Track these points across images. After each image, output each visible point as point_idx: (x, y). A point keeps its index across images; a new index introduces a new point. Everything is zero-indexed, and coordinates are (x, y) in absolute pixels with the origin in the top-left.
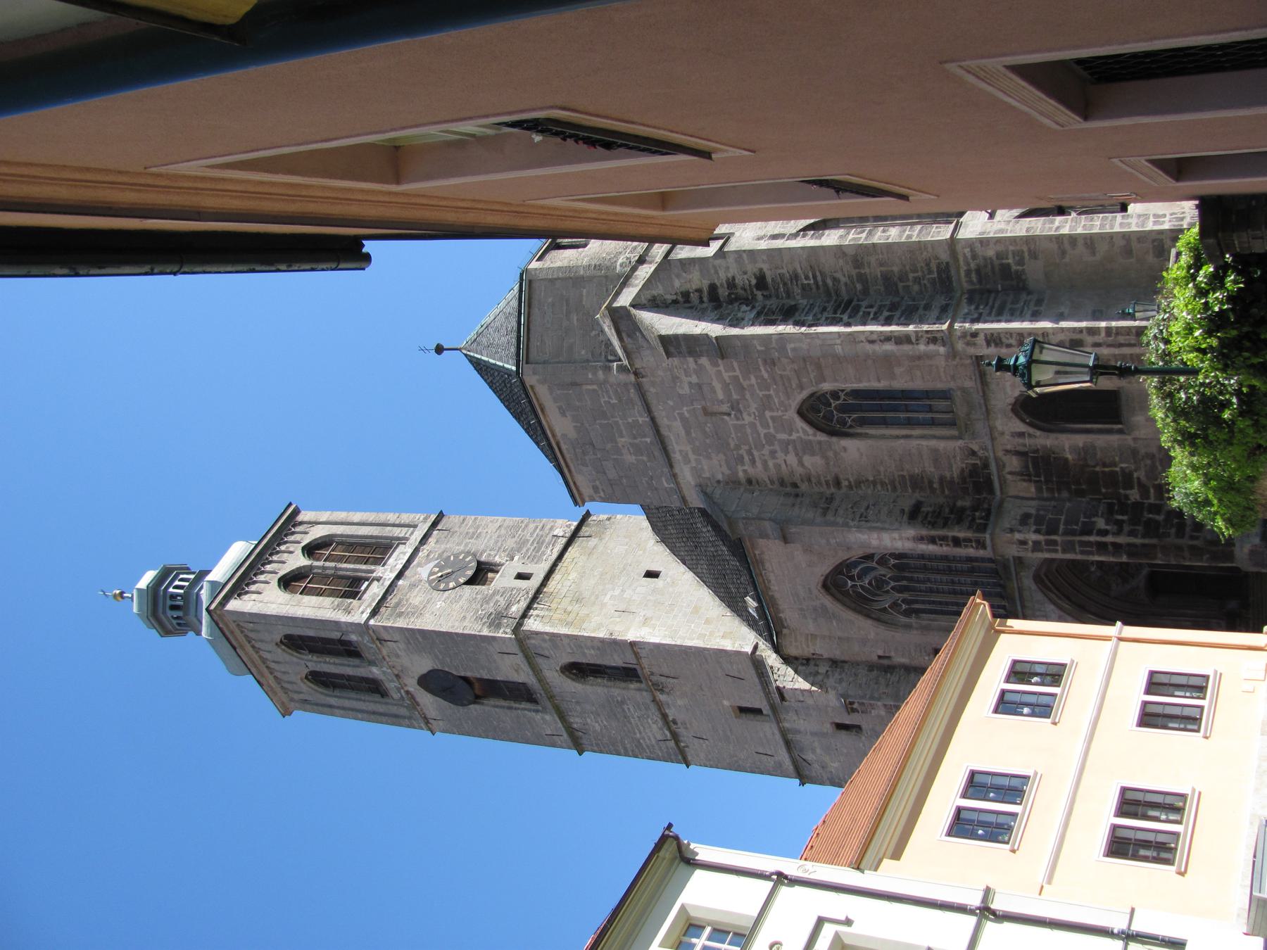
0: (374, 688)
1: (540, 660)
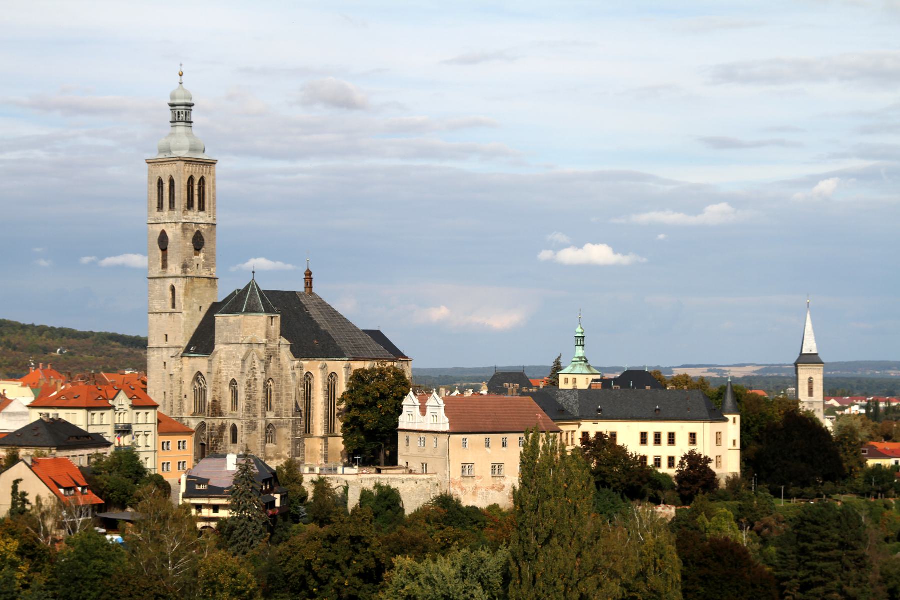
0: (160, 207)
1: (174, 280)
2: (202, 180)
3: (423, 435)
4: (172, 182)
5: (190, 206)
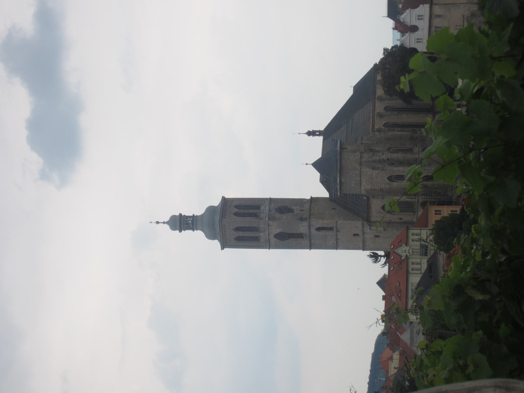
2: (236, 207)
3: (433, 29)
4: (237, 229)
5: (255, 215)
